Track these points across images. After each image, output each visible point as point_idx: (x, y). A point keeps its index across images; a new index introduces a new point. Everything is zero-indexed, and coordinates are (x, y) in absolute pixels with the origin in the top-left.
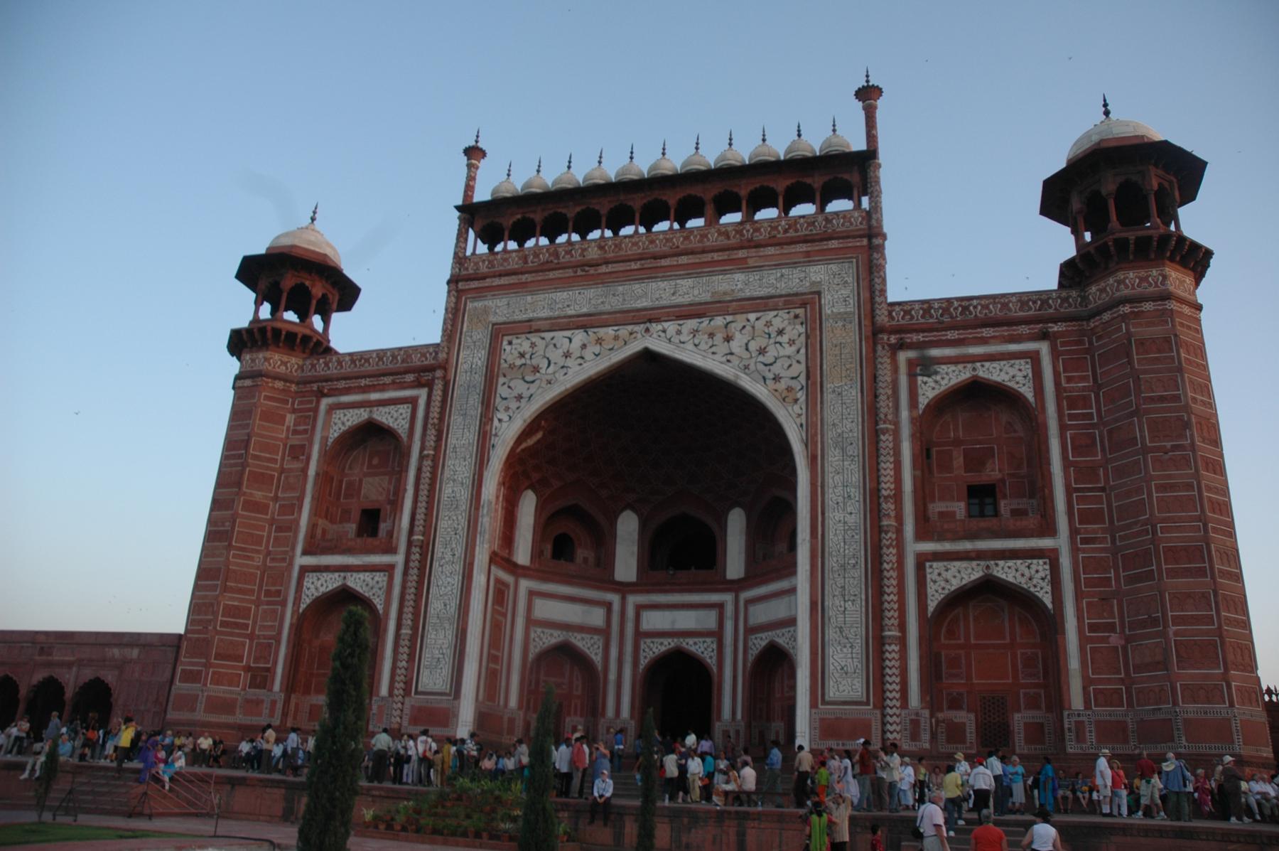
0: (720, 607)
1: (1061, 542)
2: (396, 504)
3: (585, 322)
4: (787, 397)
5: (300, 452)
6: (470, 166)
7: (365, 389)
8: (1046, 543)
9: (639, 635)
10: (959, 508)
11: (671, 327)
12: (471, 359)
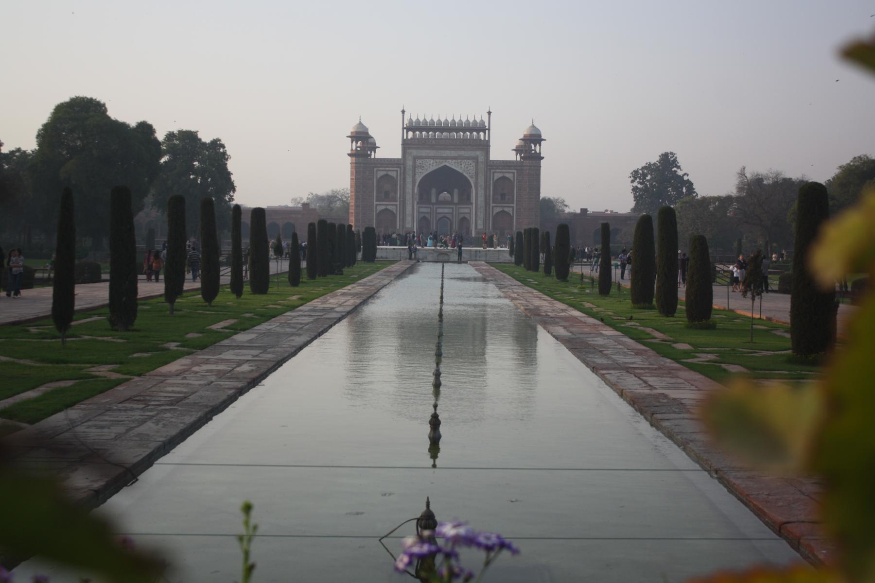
3: (433, 158)
4: (472, 177)
10: (499, 197)
12: (409, 163)
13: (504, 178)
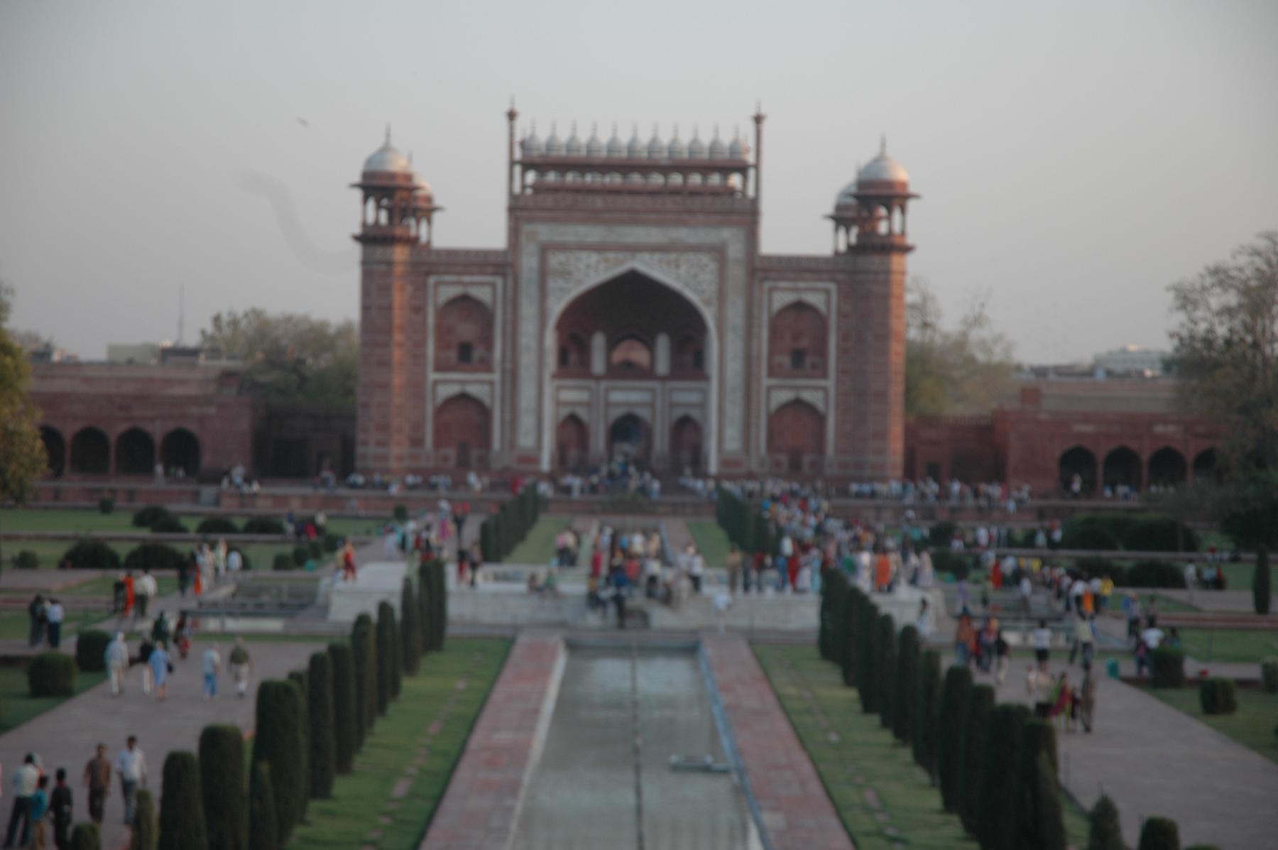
0: (653, 390)
1: (830, 383)
2: (489, 344)
5: (419, 310)
6: (512, 128)
7: (460, 274)
8: (822, 383)
9: (608, 405)
11: (646, 256)
12: (528, 263)
13: (800, 306)
